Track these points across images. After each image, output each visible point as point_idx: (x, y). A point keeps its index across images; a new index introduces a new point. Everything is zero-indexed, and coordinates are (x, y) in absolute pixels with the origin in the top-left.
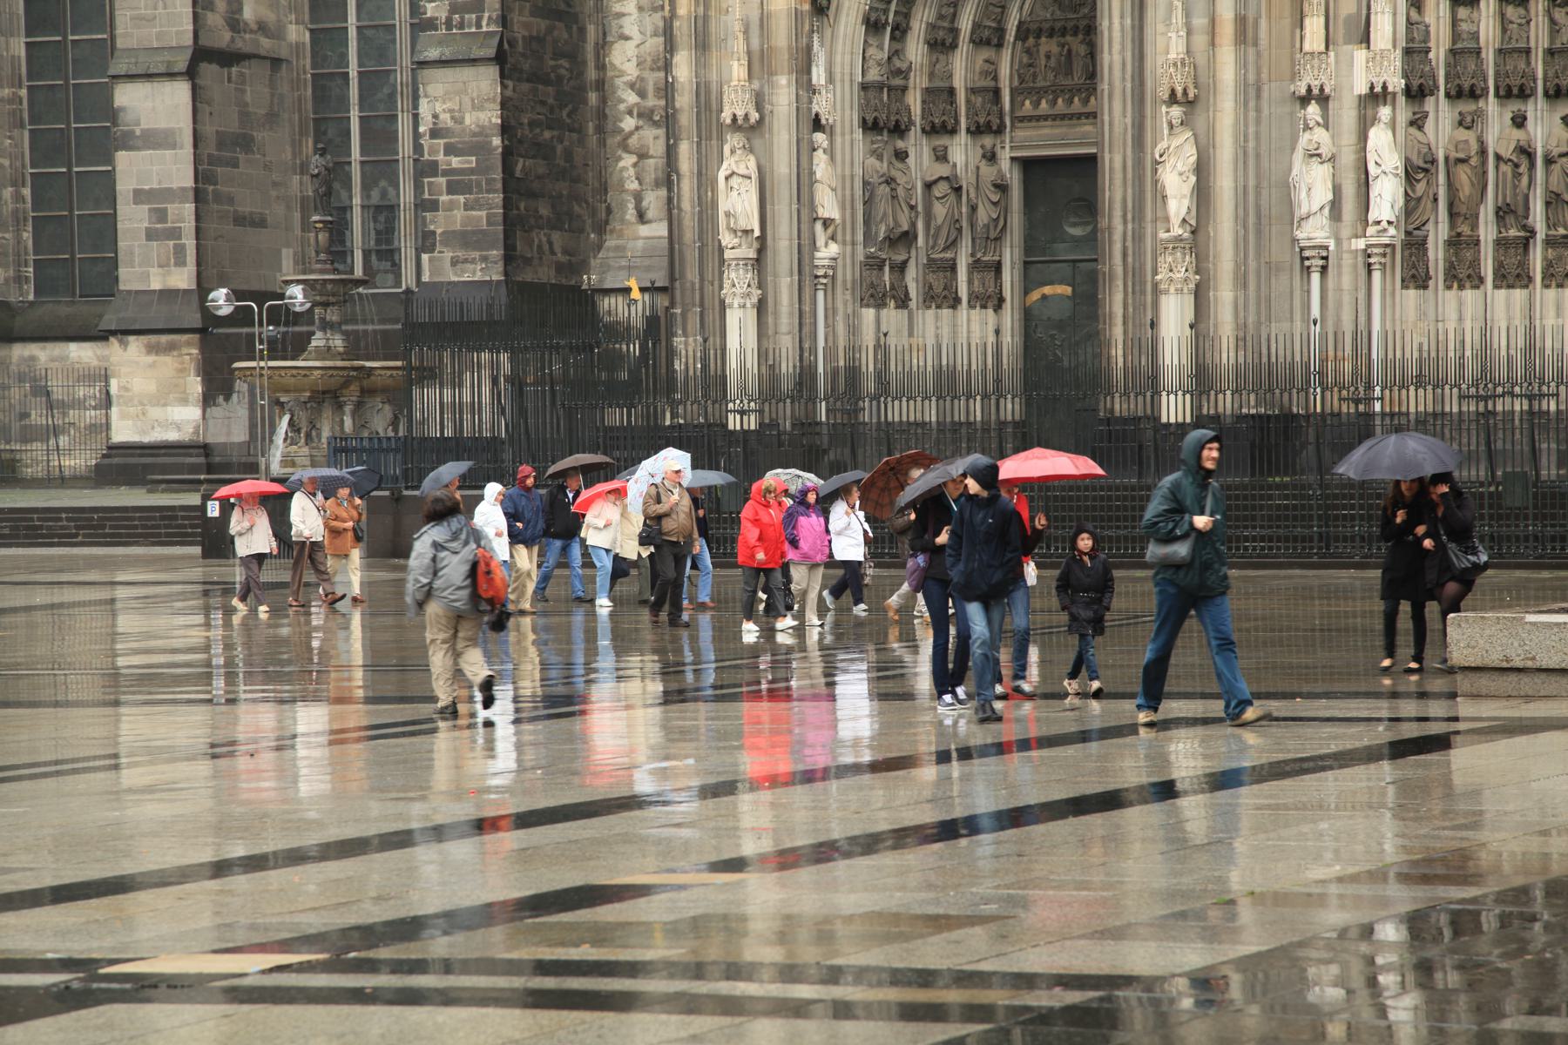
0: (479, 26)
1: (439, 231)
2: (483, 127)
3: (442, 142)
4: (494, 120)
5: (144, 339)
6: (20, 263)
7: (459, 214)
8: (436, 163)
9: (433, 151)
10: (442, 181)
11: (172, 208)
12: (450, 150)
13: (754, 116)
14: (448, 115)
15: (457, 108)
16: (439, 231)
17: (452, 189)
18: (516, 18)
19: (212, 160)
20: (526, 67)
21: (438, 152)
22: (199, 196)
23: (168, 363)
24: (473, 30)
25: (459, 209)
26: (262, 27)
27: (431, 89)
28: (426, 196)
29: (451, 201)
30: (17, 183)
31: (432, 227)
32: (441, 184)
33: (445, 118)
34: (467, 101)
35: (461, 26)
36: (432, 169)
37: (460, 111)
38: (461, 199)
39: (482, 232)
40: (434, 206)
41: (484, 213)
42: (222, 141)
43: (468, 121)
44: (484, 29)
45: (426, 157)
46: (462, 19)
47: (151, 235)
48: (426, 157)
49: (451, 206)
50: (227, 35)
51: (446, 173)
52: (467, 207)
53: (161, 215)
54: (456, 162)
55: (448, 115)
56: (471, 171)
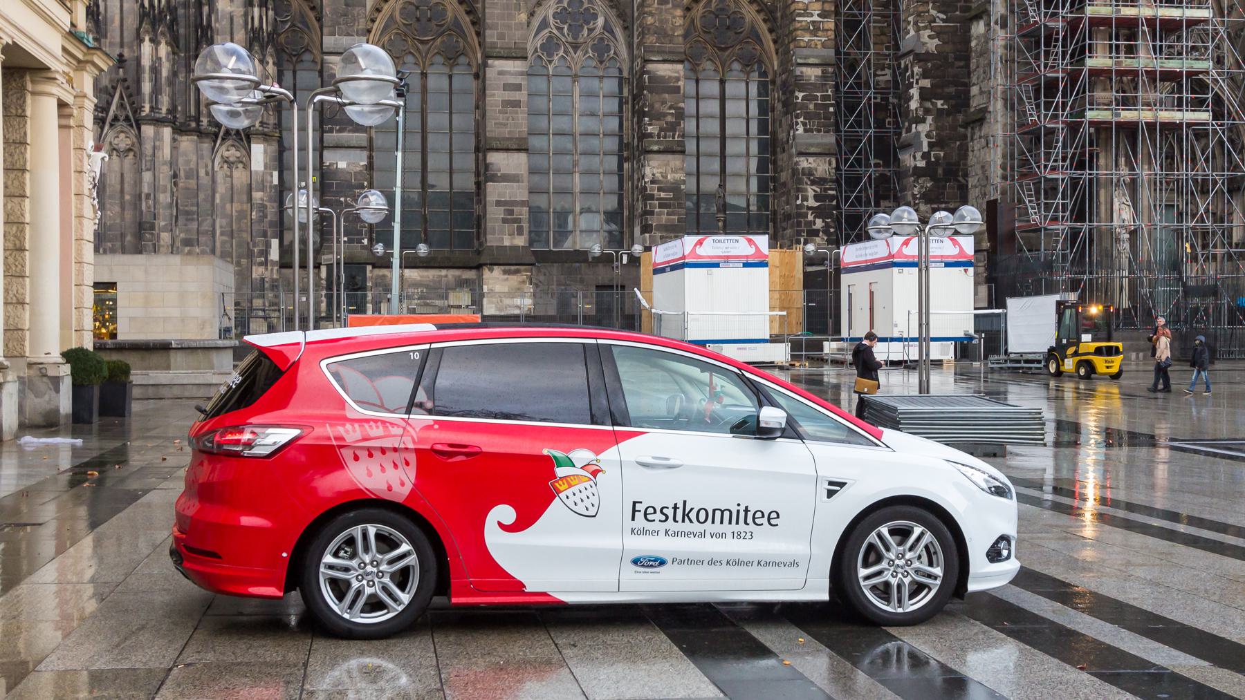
0: (673, 137)
1: (654, 224)
3: (656, 186)
5: (503, 267)
7: (664, 217)
12: (660, 190)
16: (654, 224)
17: (661, 206)
23: (514, 280)
27: (651, 163)
33: (658, 176)
34: (669, 169)
35: (665, 137)
36: (652, 197)
38: (666, 210)
39: (675, 225)
40: (652, 213)
43: (669, 177)
45: (648, 192)
46: (665, 134)
48: (648, 192)
49: (660, 214)
51: (657, 199)
54: (663, 195)
56: (671, 199)
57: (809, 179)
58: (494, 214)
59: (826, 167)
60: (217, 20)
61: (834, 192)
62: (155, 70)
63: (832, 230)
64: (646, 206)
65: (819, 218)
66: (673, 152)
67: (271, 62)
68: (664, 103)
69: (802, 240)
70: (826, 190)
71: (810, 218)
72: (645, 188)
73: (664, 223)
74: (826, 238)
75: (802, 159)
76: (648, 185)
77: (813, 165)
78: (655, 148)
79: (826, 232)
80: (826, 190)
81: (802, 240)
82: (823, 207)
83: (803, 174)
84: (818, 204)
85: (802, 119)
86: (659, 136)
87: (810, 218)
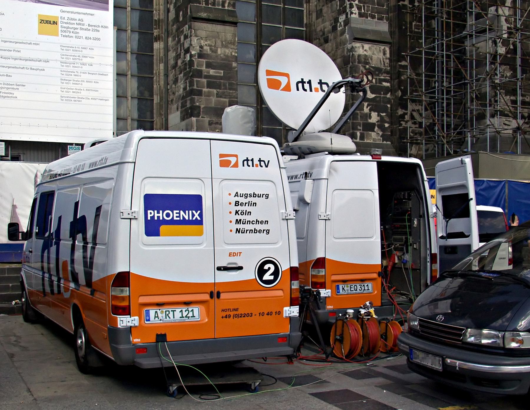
0: (223, 6)
2: (227, 56)
4: (233, 54)
7: (214, 99)
8: (201, 71)
10: (205, 81)
12: (209, 65)
14: (208, 48)
15: (213, 45)
16: (202, 106)
17: (210, 85)
21: (202, 65)
24: (220, 7)
25: (213, 96)
28: (195, 87)
29: (209, 92)
31: (198, 104)
32: (203, 82)
34: (219, 43)
36: (199, 74)
37: (215, 46)
38: (215, 91)
40: (200, 93)
41: (227, 100)
43: (219, 51)
44: (226, 8)
45: (195, 67)
48: (195, 67)
49: (209, 95)
51: (206, 77)
52: (218, 95)
54: (212, 72)
55: (208, 48)
56: (221, 78)
57: (365, 67)
59: (381, 55)
61: (388, 84)
63: (387, 125)
64: (191, 84)
65: (375, 111)
66: (224, 22)
69: (358, 134)
70: (381, 81)
71: (366, 110)
72: (191, 62)
73: (213, 105)
74: (381, 133)
75: (357, 45)
76: (195, 60)
77: (369, 53)
78: (204, 15)
79: (381, 127)
80: (381, 81)
81: (358, 134)
82: (378, 99)
83: (359, 62)
84: (374, 96)
85: (357, 2)
87: (366, 110)
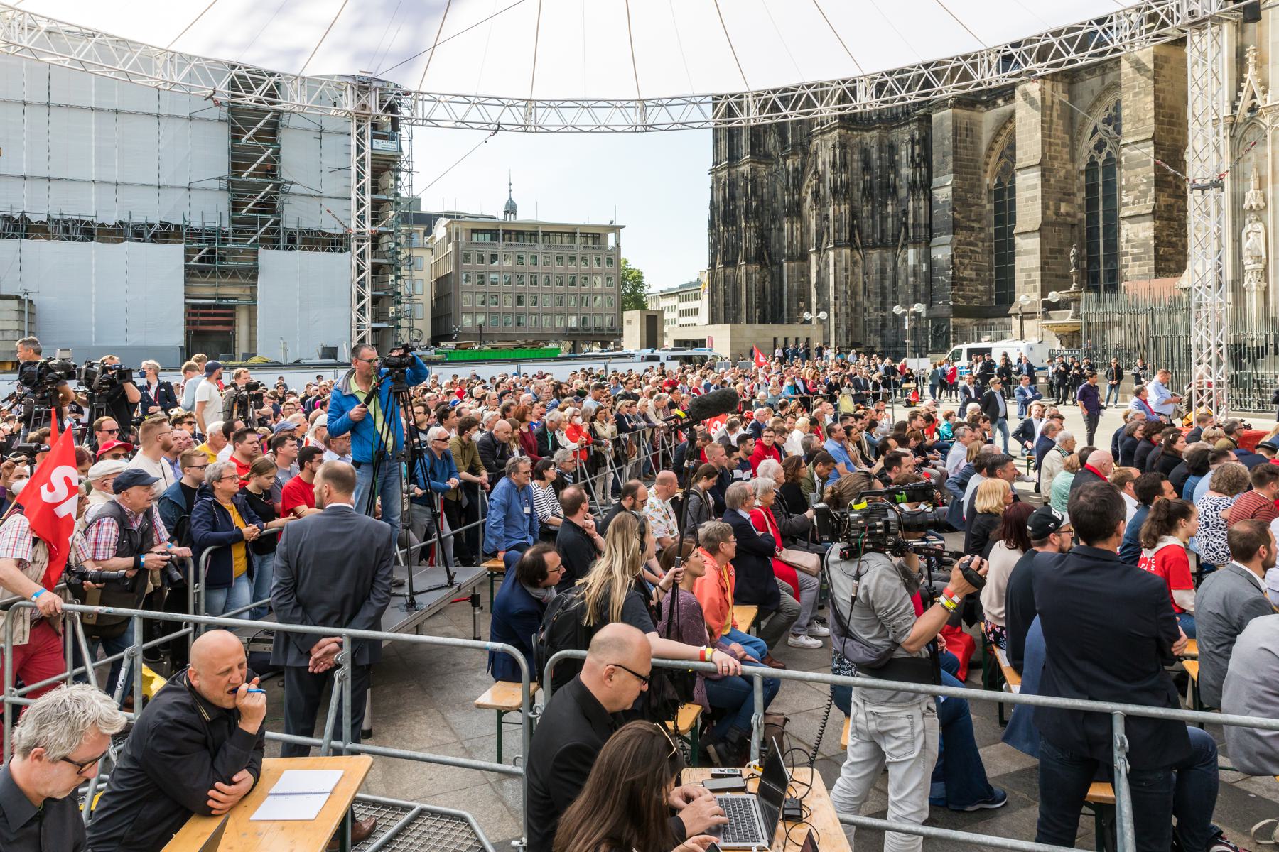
6: (991, 294)
7: (1137, 269)
9: (1127, 247)
10: (1130, 257)
11: (1033, 273)
12: (1133, 246)
13: (1262, 204)
17: (1134, 260)
18: (1161, 198)
19: (1047, 257)
20: (1165, 215)
22: (1042, 269)
26: (1068, 214)
30: (990, 270)
36: (1126, 254)
40: (1127, 266)
42: (1051, 251)
47: (1026, 283)
49: (1133, 266)
50: (1054, 217)
53: (1029, 276)
54: (1135, 251)
58: (1020, 278)
60: (901, 180)
62: (837, 220)
67: (922, 197)
68: (1136, 176)
76: (1124, 244)
86: (1134, 203)
